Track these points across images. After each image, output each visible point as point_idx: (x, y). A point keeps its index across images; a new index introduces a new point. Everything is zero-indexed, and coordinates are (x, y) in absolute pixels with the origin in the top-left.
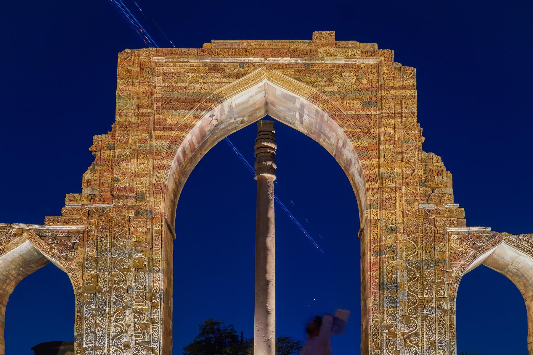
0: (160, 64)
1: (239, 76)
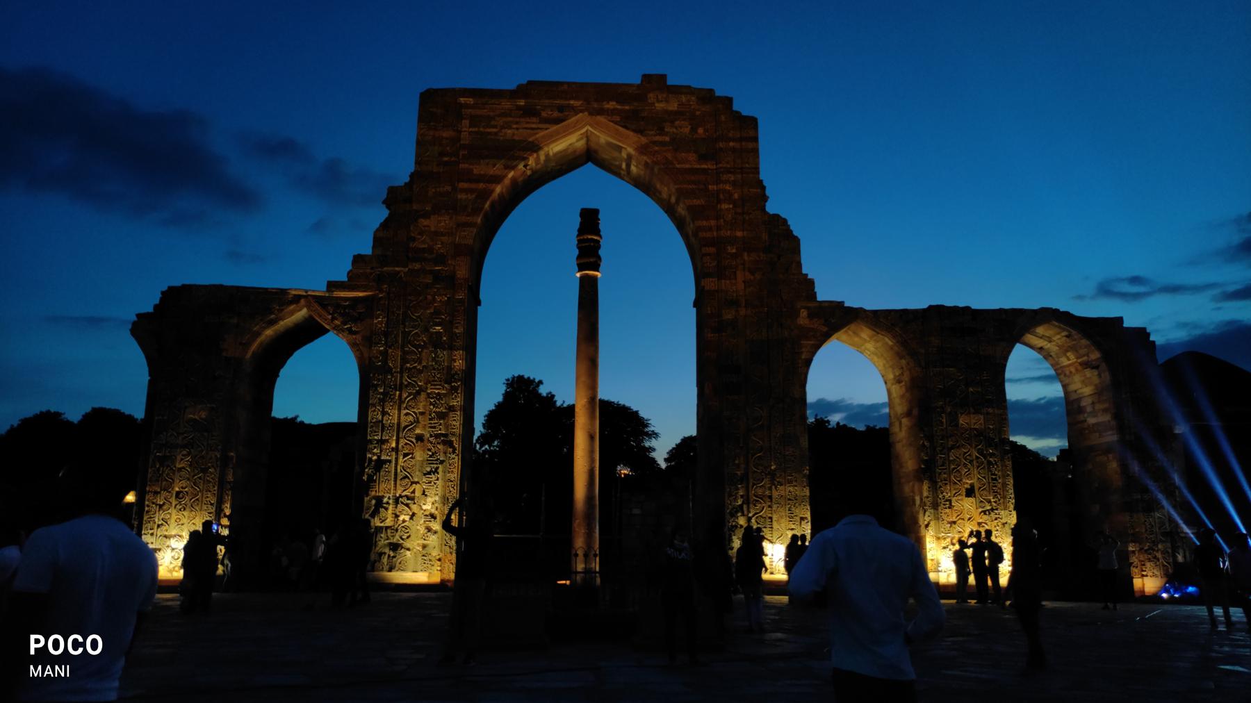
0: (467, 106)
1: (558, 121)
